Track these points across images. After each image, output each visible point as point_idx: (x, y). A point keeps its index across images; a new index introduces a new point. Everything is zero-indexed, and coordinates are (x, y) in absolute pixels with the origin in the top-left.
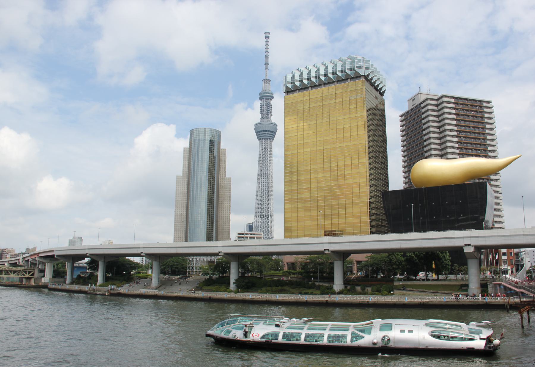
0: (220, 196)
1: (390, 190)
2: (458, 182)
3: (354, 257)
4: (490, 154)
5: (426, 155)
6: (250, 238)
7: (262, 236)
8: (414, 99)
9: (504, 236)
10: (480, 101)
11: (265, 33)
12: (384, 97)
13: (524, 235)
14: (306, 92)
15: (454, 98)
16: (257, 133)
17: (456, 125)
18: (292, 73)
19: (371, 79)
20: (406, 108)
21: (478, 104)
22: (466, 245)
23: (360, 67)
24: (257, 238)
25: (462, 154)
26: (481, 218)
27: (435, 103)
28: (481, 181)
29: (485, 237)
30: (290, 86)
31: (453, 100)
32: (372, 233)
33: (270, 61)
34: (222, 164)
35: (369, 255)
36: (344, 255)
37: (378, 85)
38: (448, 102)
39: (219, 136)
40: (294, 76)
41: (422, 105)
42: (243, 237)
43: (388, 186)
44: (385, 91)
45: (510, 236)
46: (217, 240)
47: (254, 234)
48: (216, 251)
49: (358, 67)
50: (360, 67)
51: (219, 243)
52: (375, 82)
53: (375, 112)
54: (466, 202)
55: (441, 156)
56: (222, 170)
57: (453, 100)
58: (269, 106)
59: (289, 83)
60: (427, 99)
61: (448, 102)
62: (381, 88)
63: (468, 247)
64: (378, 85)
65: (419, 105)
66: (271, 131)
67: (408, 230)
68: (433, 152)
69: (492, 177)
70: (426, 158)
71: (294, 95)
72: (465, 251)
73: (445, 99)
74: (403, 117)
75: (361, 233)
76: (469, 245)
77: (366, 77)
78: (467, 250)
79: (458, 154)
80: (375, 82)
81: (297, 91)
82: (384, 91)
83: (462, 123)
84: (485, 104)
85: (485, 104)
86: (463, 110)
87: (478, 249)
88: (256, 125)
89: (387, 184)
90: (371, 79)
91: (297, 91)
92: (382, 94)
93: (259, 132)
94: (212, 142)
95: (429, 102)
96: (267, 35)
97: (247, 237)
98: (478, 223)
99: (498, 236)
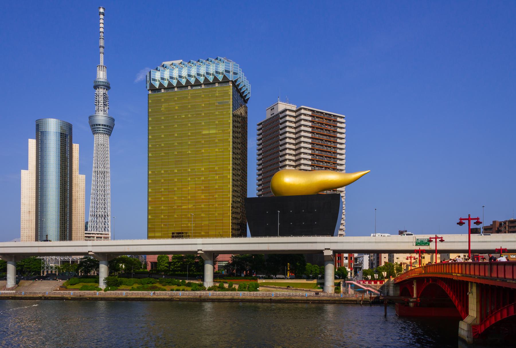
0: (74, 194)
1: (248, 196)
6: (97, 237)
7: (110, 236)
9: (359, 242)
10: (334, 116)
13: (376, 242)
21: (333, 118)
22: (326, 249)
27: (294, 114)
29: (343, 242)
36: (213, 255)
38: (305, 115)
41: (281, 116)
45: (364, 242)
46: (70, 239)
47: (101, 234)
53: (239, 120)
60: (286, 110)
61: (305, 115)
63: (327, 251)
65: (278, 114)
67: (274, 234)
72: (325, 254)
78: (326, 253)
83: (317, 136)
84: (339, 119)
86: (318, 123)
87: (335, 252)
95: (288, 113)
97: (94, 237)
98: (330, 229)
99: (354, 242)
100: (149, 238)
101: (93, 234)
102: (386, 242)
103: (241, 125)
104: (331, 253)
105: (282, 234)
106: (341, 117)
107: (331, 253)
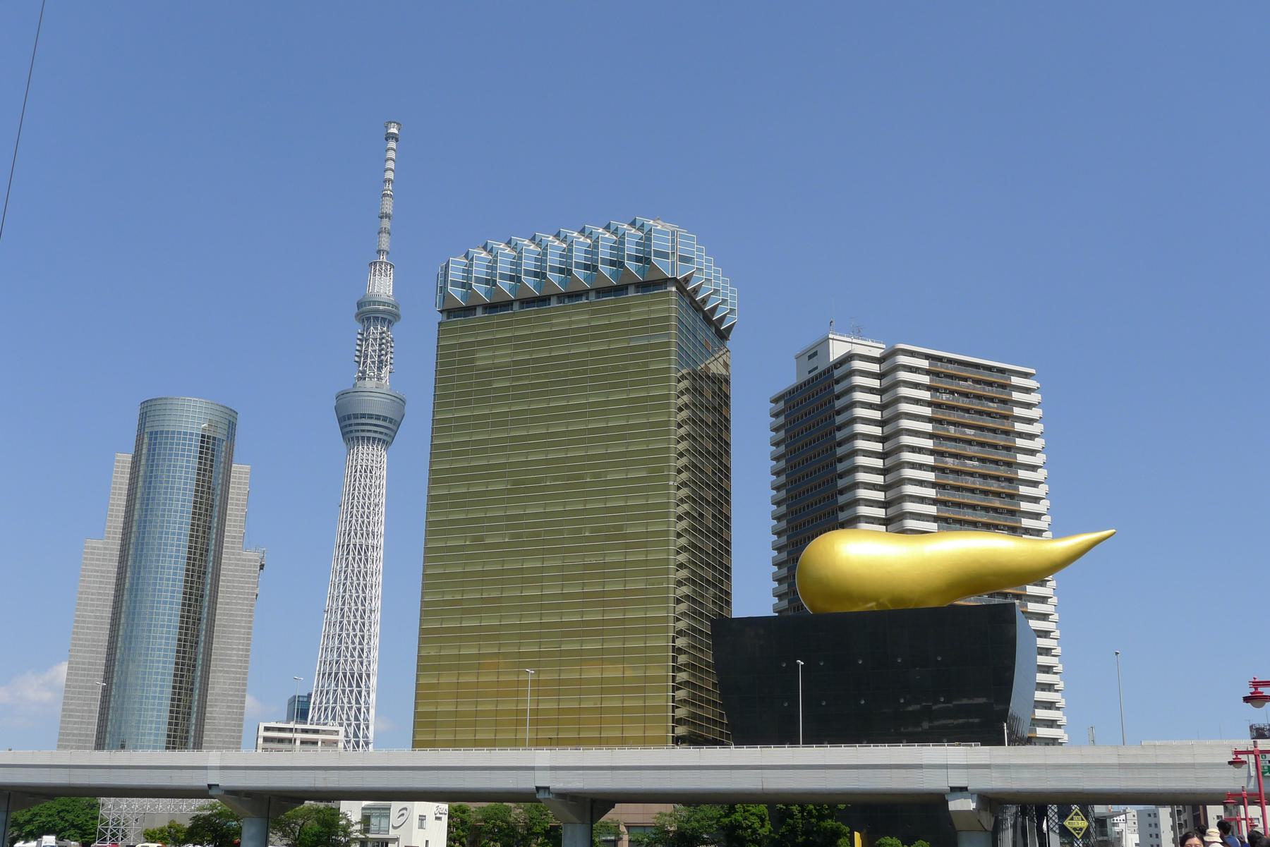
2: (934, 603)
3: (621, 814)
4: (1026, 523)
5: (842, 516)
6: (302, 742)
7: (341, 737)
8: (815, 354)
10: (1002, 371)
12: (728, 344)
15: (927, 357)
17: (931, 436)
19: (696, 291)
20: (789, 378)
22: (953, 789)
23: (665, 255)
24: (323, 742)
25: (946, 520)
26: (997, 708)
27: (875, 368)
28: (997, 601)
30: (456, 293)
31: (924, 364)
32: (677, 741)
35: (668, 808)
37: (714, 310)
39: (232, 426)
41: (837, 373)
42: (281, 740)
43: (728, 603)
44: (731, 327)
46: (198, 746)
47: (316, 732)
48: (200, 781)
49: (658, 254)
50: (665, 255)
51: (211, 757)
52: (704, 301)
54: (953, 660)
55: (886, 522)
57: (924, 364)
59: (454, 284)
60: (850, 357)
62: (722, 319)
63: (959, 794)
64: (714, 310)
66: (385, 419)
67: (786, 737)
68: (864, 510)
69: (1031, 590)
70: (843, 525)
71: (470, 321)
73: (903, 360)
74: (781, 404)
75: (645, 742)
76: (964, 789)
77: (681, 285)
78: (958, 805)
79: (935, 519)
80: (704, 301)
82: (730, 328)
84: (1015, 380)
85: (1015, 380)
87: (992, 802)
88: (341, 396)
89: (725, 598)
90: (696, 291)
92: (723, 336)
95: (858, 365)
100: (417, 744)
101: (291, 730)
102: (1157, 766)
103: (712, 399)
104: (970, 805)
105: (817, 736)
106: (1026, 375)
107: (970, 805)
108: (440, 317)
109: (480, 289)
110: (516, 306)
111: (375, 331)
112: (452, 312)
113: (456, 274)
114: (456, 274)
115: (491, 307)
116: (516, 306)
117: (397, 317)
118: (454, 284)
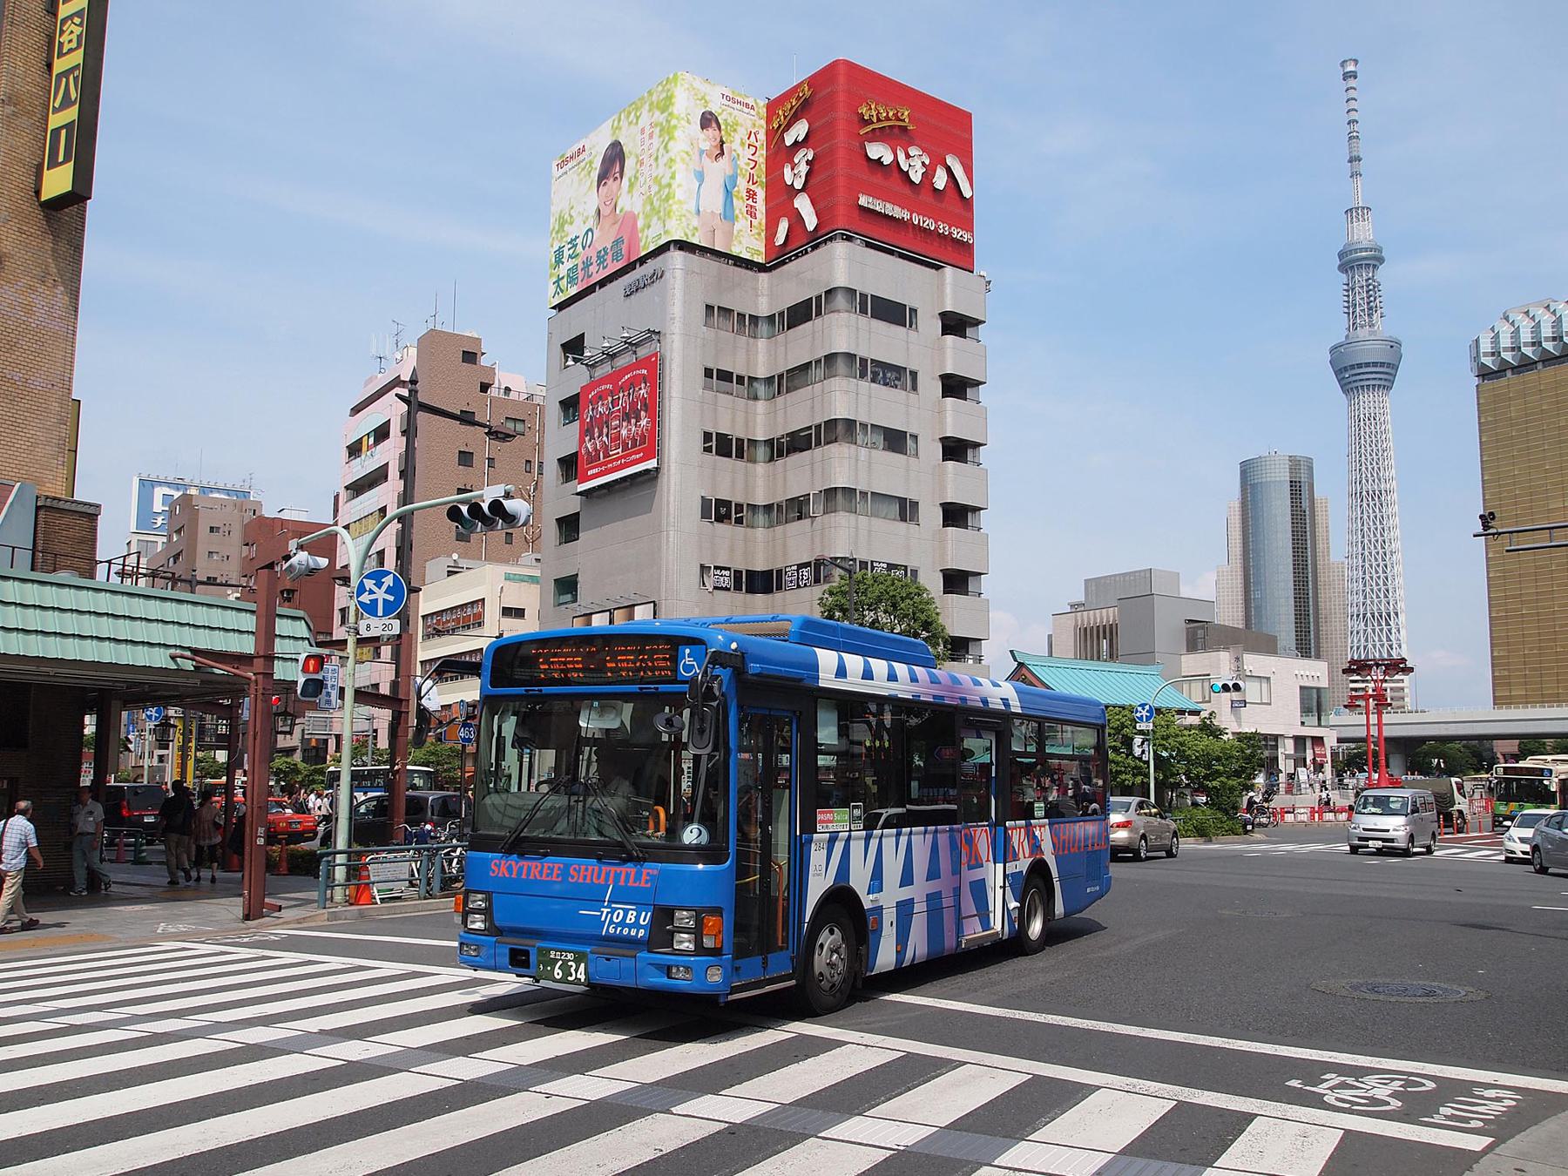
11: (1343, 64)
14: (1530, 376)
16: (1339, 372)
18: (1493, 329)
30: (1488, 361)
33: (1362, 149)
34: (1320, 531)
39: (1311, 469)
40: (1497, 336)
56: (1320, 546)
58: (1372, 289)
59: (1486, 354)
66: (1382, 364)
81: (1509, 373)
88: (1333, 350)
91: (1509, 373)
93: (1346, 369)
94: (1296, 488)
96: (1350, 68)
108: (1476, 381)
109: (1508, 356)
110: (1540, 366)
111: (1360, 278)
112: (1485, 374)
113: (1486, 346)
114: (1486, 346)
115: (1516, 369)
116: (1540, 366)
117: (1381, 260)
118: (1486, 354)
